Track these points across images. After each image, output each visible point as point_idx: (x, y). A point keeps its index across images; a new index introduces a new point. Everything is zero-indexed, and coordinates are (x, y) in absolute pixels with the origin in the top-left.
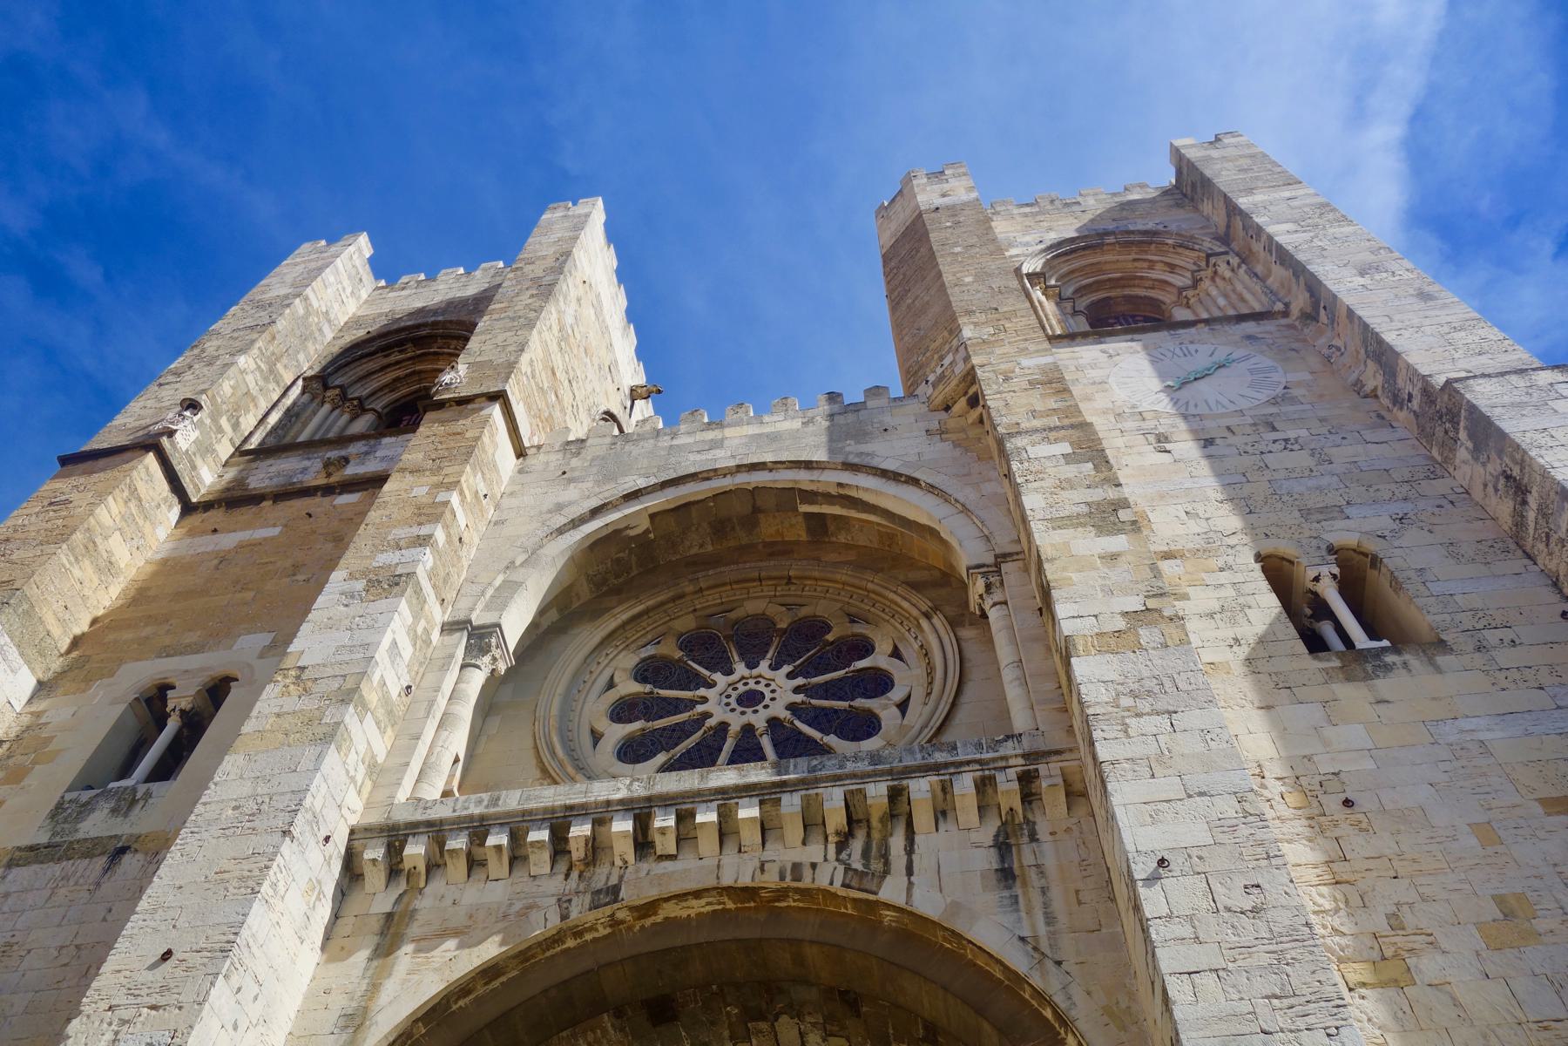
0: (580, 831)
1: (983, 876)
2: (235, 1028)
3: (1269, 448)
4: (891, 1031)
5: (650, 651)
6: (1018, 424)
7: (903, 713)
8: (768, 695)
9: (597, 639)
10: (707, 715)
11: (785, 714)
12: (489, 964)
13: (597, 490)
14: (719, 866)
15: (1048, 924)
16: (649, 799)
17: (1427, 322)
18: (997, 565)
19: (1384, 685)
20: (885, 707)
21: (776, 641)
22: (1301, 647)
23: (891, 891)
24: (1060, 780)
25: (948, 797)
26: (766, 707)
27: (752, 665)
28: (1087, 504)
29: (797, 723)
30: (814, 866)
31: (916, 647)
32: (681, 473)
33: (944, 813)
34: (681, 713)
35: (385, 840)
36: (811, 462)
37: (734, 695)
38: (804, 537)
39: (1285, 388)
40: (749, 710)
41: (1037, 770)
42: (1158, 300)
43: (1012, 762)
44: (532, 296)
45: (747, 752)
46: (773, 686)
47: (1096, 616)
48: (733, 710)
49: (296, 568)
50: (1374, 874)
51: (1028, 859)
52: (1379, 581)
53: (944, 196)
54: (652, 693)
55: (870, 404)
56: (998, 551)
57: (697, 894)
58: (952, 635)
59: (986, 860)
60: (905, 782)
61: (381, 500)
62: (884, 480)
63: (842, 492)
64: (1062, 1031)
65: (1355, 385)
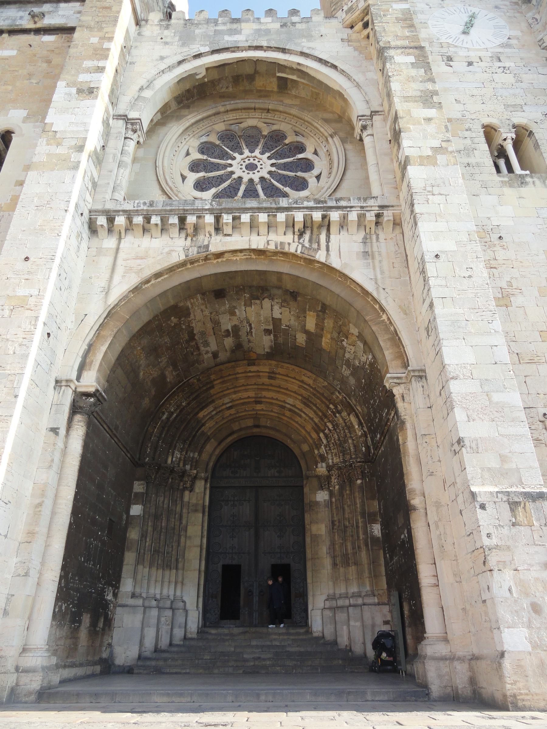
0: (191, 219)
1: (357, 254)
2: (61, 289)
3: (497, 71)
4: (307, 307)
5: (204, 139)
6: (389, 42)
7: (318, 181)
8: (259, 167)
9: (181, 131)
10: (232, 173)
11: (267, 176)
12: (157, 272)
13: (180, 51)
14: (249, 241)
15: (381, 274)
16: (221, 209)
18: (371, 116)
19: (524, 191)
20: (311, 177)
21: (262, 141)
22: (494, 170)
23: (321, 256)
24: (392, 218)
25: (345, 220)
26: (258, 171)
27: (252, 151)
28: (422, 91)
29: (272, 180)
30: (289, 244)
31: (325, 150)
33: (342, 227)
34: (220, 170)
35: (105, 217)
36: (285, 49)
37: (244, 164)
38: (276, 89)
39: (509, 38)
40: (251, 172)
41: (383, 213)
43: (373, 209)
45: (251, 192)
46: (261, 162)
47: (420, 147)
48: (244, 172)
49: (30, 75)
50: (505, 266)
51: (375, 249)
52: (528, 143)
54: (207, 160)
55: (314, 19)
56: (373, 109)
57: (241, 251)
58: (342, 147)
59: (358, 247)
60: (329, 213)
61: (74, 43)
62: (320, 64)
63: (299, 67)
64: (381, 313)
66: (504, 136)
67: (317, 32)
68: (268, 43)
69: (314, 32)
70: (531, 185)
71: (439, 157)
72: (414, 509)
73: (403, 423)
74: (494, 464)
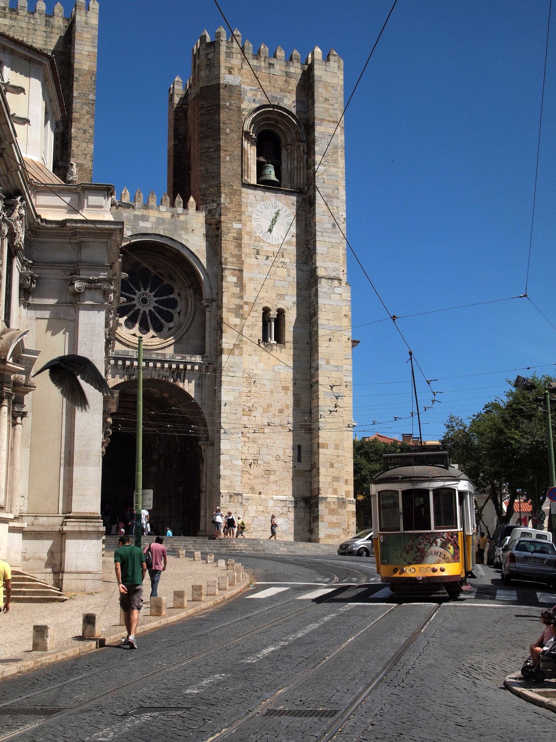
0: (128, 363)
8: (149, 301)
11: (153, 310)
17: (329, 240)
20: (176, 313)
24: (212, 370)
26: (148, 305)
27: (145, 290)
28: (236, 305)
29: (155, 313)
30: (168, 377)
32: (138, 233)
39: (292, 236)
42: (280, 137)
44: (88, 113)
46: (150, 298)
48: (140, 304)
53: (230, 73)
65: (308, 241)
66: (271, 316)
67: (191, 225)
68: (164, 232)
69: (188, 226)
70: (275, 351)
71: (236, 350)
72: (203, 492)
73: (203, 461)
74: (229, 484)
